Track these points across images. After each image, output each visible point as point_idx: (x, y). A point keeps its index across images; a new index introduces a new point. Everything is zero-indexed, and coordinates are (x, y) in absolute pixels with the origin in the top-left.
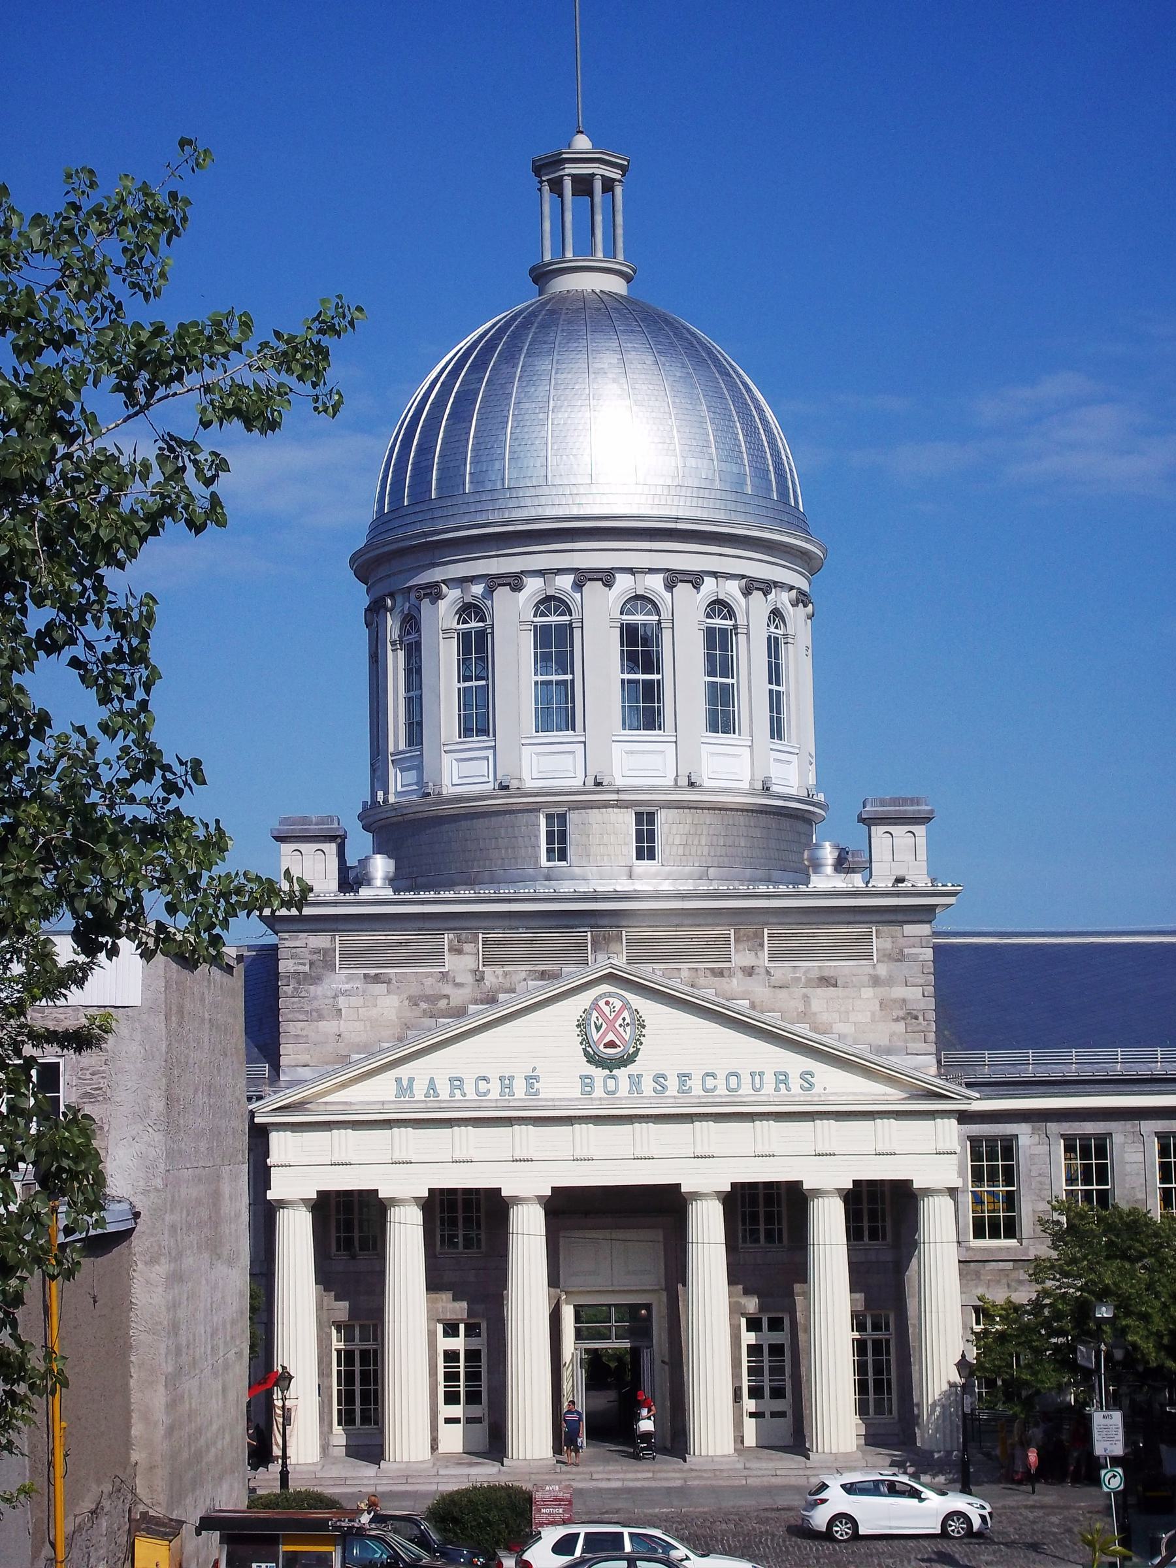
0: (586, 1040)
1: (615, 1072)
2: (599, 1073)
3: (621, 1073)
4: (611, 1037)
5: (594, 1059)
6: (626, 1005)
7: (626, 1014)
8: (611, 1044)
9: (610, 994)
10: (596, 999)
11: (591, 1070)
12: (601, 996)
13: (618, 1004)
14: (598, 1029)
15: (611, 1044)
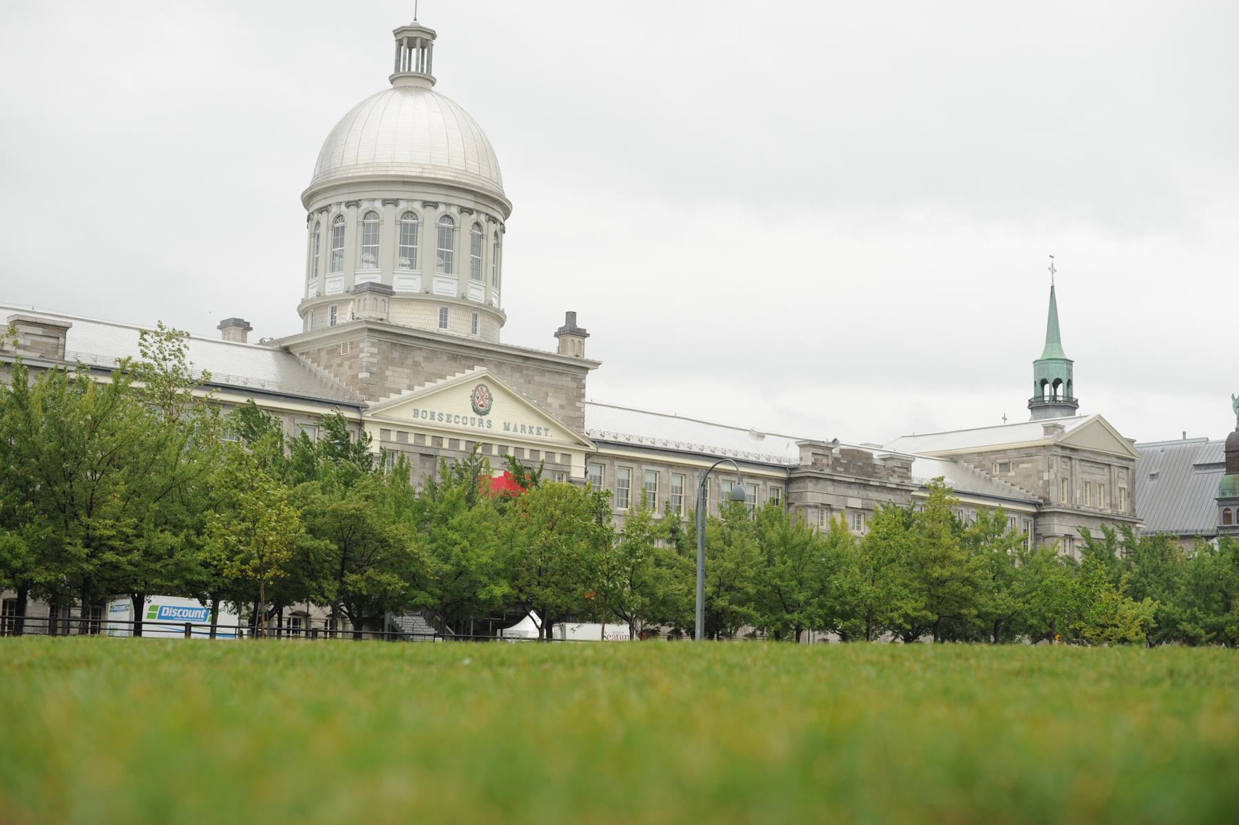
0: (474, 404)
1: (483, 417)
2: (478, 417)
3: (485, 418)
4: (482, 402)
5: (476, 411)
6: (488, 391)
7: (487, 394)
8: (482, 406)
9: (482, 385)
10: (478, 386)
11: (474, 415)
12: (480, 385)
13: (485, 389)
14: (478, 398)
15: (482, 406)
